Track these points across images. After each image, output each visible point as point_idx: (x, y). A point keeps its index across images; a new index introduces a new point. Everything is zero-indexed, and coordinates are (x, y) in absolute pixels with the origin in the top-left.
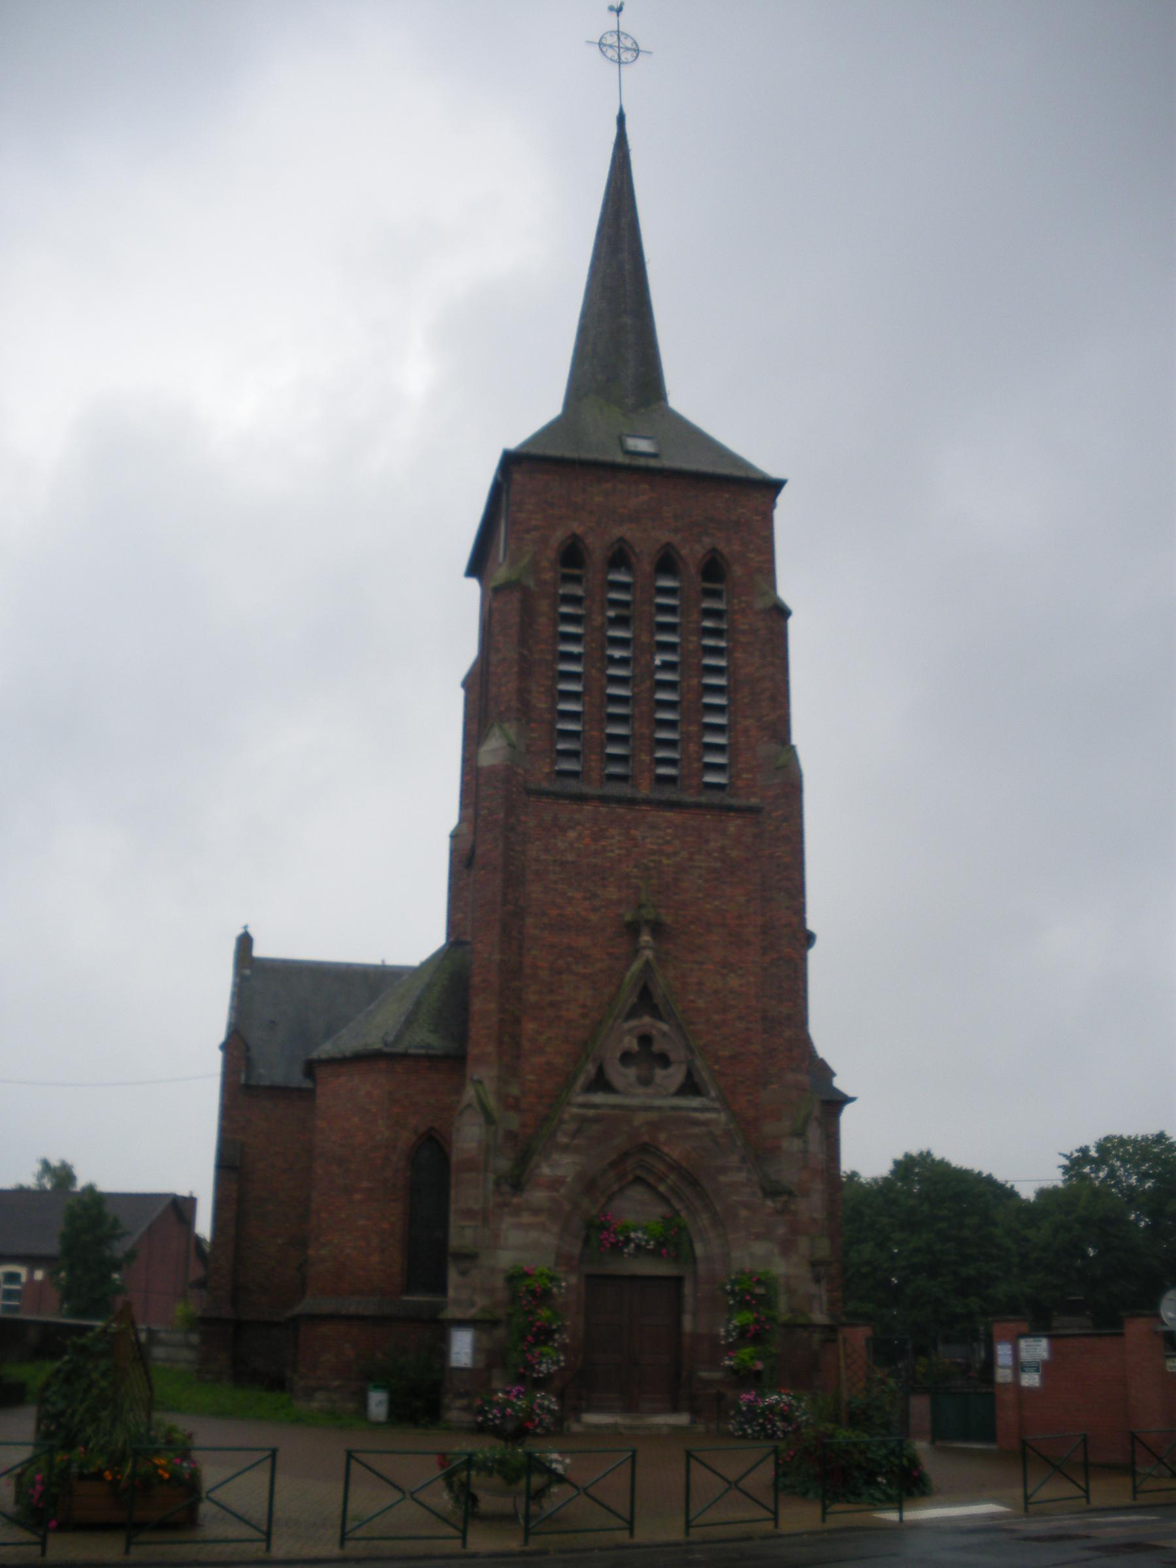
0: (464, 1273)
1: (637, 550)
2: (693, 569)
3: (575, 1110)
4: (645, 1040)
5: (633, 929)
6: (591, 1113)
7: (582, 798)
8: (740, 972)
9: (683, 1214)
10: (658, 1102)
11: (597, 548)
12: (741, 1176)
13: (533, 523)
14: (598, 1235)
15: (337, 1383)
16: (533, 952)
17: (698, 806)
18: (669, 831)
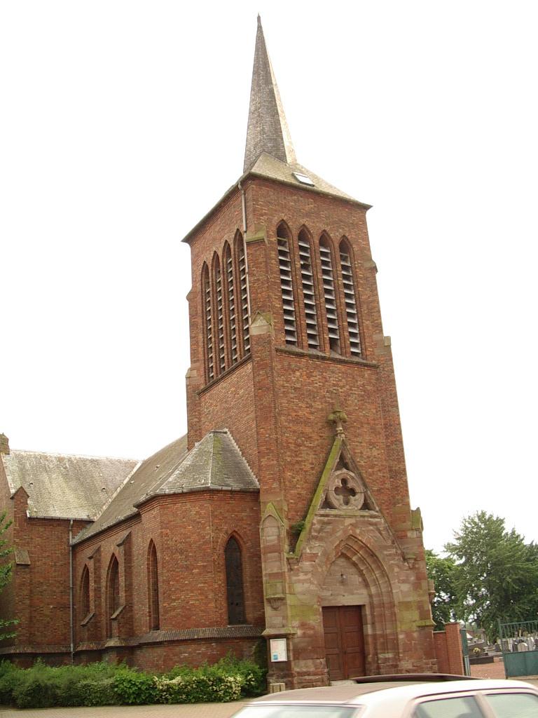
2: (337, 245)
4: (344, 481)
5: (332, 424)
8: (378, 447)
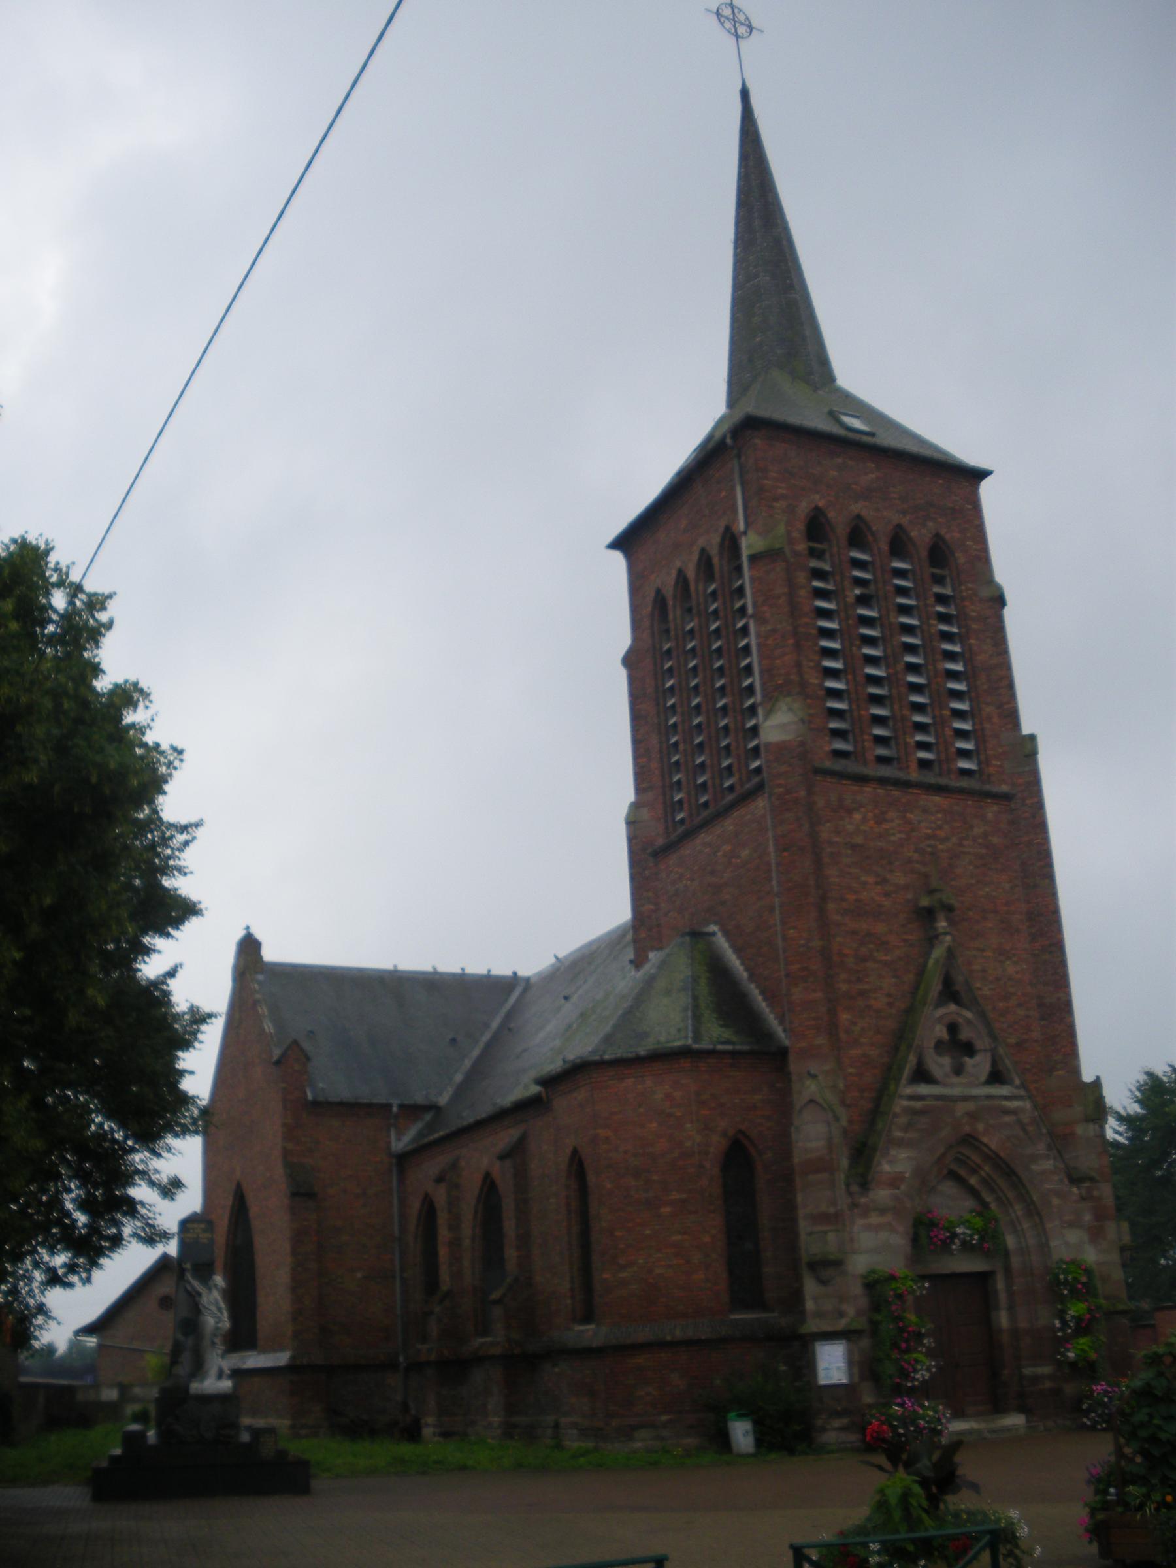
0: (823, 1282)
1: (874, 528)
2: (924, 553)
3: (905, 1103)
4: (953, 1028)
5: (928, 915)
6: (918, 1105)
7: (862, 779)
8: (1015, 959)
9: (993, 1206)
10: (976, 1092)
11: (839, 520)
12: (1048, 1164)
13: (780, 491)
14: (926, 1233)
15: (664, 1418)
16: (838, 939)
17: (961, 791)
18: (939, 815)
